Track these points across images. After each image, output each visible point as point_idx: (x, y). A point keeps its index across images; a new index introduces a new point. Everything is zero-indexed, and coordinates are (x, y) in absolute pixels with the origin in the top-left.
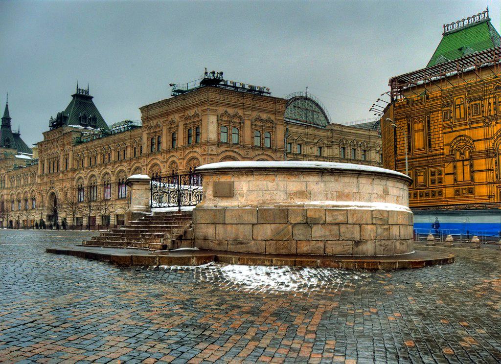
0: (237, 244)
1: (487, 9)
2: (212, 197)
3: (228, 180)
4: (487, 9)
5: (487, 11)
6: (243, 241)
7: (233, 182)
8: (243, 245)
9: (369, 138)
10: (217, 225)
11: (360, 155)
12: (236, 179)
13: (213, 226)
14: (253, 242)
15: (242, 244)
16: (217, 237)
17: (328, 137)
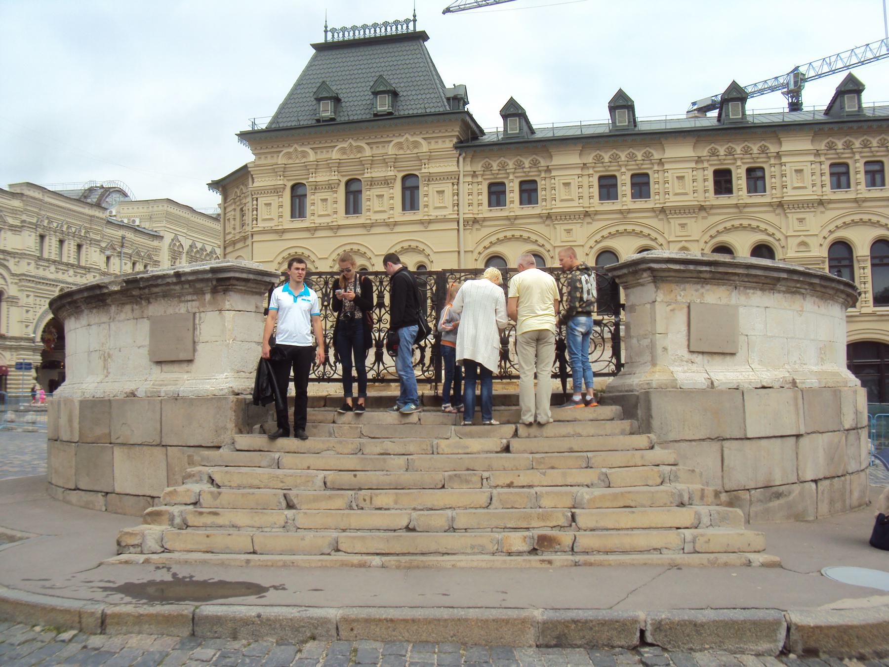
0: (770, 500)
1: (415, 16)
2: (684, 352)
3: (724, 301)
4: (415, 16)
5: (415, 21)
6: (781, 489)
7: (736, 307)
8: (782, 501)
9: (91, 220)
10: (726, 444)
11: (69, 253)
12: (743, 299)
13: (716, 446)
14: (797, 488)
15: (778, 496)
16: (726, 481)
17: (14, 212)
